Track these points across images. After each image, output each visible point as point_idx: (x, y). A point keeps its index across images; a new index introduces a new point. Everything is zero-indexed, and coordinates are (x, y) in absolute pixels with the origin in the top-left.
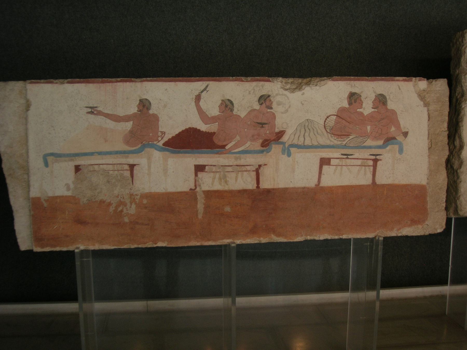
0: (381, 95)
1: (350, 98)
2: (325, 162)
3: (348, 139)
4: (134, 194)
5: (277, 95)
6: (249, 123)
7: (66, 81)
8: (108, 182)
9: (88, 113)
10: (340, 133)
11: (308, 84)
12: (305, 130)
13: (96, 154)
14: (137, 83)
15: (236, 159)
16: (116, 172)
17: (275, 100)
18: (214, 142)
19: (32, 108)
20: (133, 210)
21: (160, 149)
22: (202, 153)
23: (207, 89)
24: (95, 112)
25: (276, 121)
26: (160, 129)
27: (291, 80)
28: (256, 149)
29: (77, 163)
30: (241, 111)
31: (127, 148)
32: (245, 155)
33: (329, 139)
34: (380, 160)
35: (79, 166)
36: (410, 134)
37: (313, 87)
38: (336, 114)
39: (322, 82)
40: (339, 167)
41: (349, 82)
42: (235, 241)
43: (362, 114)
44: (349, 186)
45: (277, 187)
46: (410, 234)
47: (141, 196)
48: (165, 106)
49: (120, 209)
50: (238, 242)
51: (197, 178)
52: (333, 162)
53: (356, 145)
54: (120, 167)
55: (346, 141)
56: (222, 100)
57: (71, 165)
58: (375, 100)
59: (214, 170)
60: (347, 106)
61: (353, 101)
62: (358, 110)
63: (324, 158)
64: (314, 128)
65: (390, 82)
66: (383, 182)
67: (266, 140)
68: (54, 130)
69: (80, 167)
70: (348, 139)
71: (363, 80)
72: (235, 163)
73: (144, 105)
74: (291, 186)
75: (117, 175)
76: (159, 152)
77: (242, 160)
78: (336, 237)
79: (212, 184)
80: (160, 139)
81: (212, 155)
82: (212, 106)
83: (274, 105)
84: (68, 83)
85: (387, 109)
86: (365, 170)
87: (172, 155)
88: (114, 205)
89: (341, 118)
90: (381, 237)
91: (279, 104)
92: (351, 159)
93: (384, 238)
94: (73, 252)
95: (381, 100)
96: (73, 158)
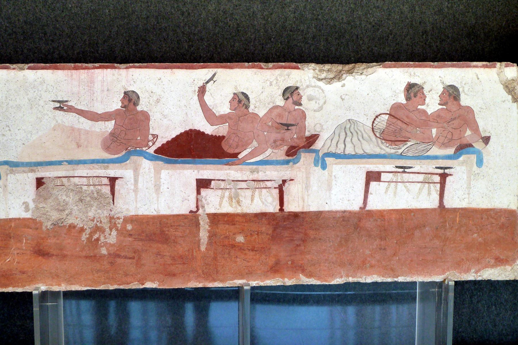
1: (408, 91)
2: (372, 177)
3: (405, 147)
4: (115, 217)
5: (308, 87)
6: (270, 124)
7: (27, 66)
8: (81, 200)
9: (56, 108)
10: (393, 139)
11: (350, 72)
12: (346, 134)
13: (66, 163)
14: (121, 70)
15: (252, 172)
16: (92, 188)
17: (305, 94)
18: (222, 149)
20: (112, 238)
22: (207, 164)
23: (214, 79)
24: (65, 108)
25: (306, 123)
26: (151, 131)
27: (327, 67)
28: (278, 159)
29: (39, 175)
30: (259, 108)
31: (106, 156)
32: (264, 166)
33: (379, 146)
34: (451, 175)
35: (43, 178)
37: (357, 77)
38: (388, 112)
39: (370, 70)
40: (393, 184)
41: (406, 69)
42: (250, 282)
43: (424, 112)
44: (406, 210)
46: (494, 278)
47: (124, 219)
48: (158, 101)
49: (96, 236)
50: (254, 283)
51: (199, 196)
52: (384, 177)
53: (417, 155)
55: (402, 149)
56: (235, 94)
57: (31, 178)
58: (442, 93)
59: (222, 187)
60: (404, 101)
61: (412, 95)
62: (419, 107)
63: (371, 172)
64: (358, 131)
65: (464, 69)
66: (454, 206)
67: (292, 148)
68: (10, 130)
69: (44, 180)
71: (426, 67)
72: (251, 178)
73: (130, 99)
74: (327, 208)
75: (92, 191)
76: (149, 161)
77: (260, 173)
78: (389, 280)
79: (220, 205)
80: (150, 144)
81: (220, 166)
83: (304, 101)
84: (29, 68)
85: (460, 105)
86: (429, 188)
87: (167, 165)
88: (88, 231)
89: (396, 118)
90: (451, 281)
91: (310, 99)
92: (409, 173)
93: (456, 282)
94: (31, 294)
95: (452, 93)
96: (35, 168)
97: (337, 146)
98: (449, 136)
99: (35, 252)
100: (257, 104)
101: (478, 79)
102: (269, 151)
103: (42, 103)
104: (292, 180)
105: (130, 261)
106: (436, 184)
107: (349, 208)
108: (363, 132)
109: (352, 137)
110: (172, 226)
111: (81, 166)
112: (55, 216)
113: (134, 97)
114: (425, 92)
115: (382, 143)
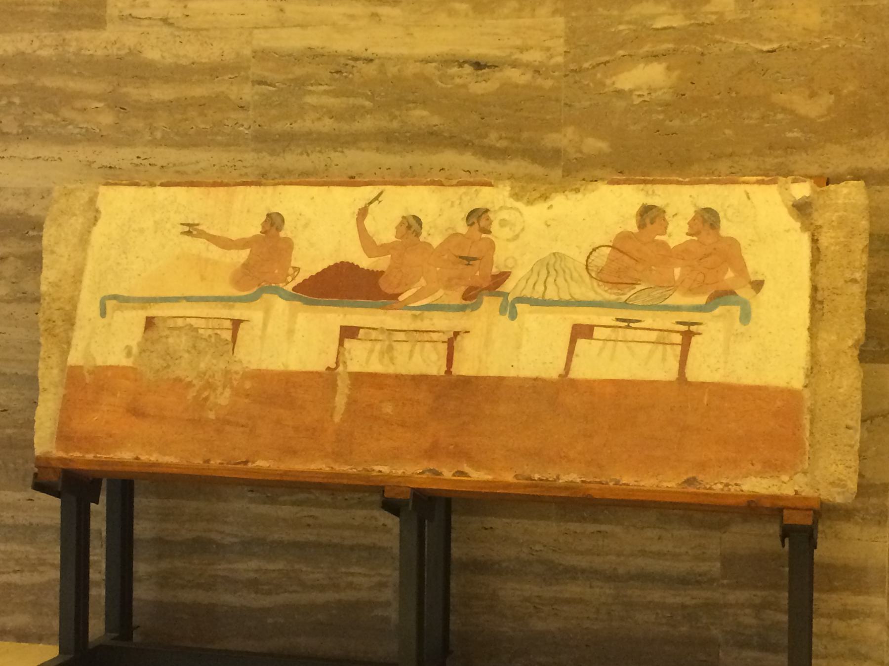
0: (708, 210)
2: (582, 332)
3: (633, 292)
5: (501, 208)
10: (616, 280)
12: (548, 272)
16: (210, 332)
17: (495, 218)
19: (100, 223)
21: (288, 297)
24: (195, 233)
25: (495, 256)
26: (293, 264)
28: (451, 303)
30: (433, 236)
34: (699, 334)
36: (765, 286)
40: (610, 344)
41: (642, 186)
43: (664, 244)
45: (486, 375)
48: (306, 226)
49: (206, 394)
52: (597, 332)
53: (649, 304)
54: (215, 323)
55: (628, 294)
56: (404, 217)
58: (694, 219)
59: (373, 337)
61: (648, 221)
62: (658, 237)
65: (728, 186)
66: (702, 379)
69: (156, 321)
70: (633, 292)
72: (412, 328)
73: (274, 222)
74: (512, 373)
75: (210, 336)
76: (284, 301)
79: (368, 361)
80: (289, 279)
82: (384, 226)
83: (495, 227)
85: (718, 235)
86: (665, 351)
89: (622, 252)
91: (503, 223)
92: (635, 328)
95: (708, 219)
97: (534, 288)
98: (700, 278)
99: (128, 411)
100: (432, 231)
101: (749, 198)
102: (441, 293)
103: (168, 226)
104: (466, 332)
105: (242, 429)
106: (675, 346)
107: (544, 375)
108: (573, 269)
109: (557, 276)
110: (301, 386)
111: (203, 304)
112: (157, 363)
113: (278, 220)
114: (667, 217)
115: (598, 285)
